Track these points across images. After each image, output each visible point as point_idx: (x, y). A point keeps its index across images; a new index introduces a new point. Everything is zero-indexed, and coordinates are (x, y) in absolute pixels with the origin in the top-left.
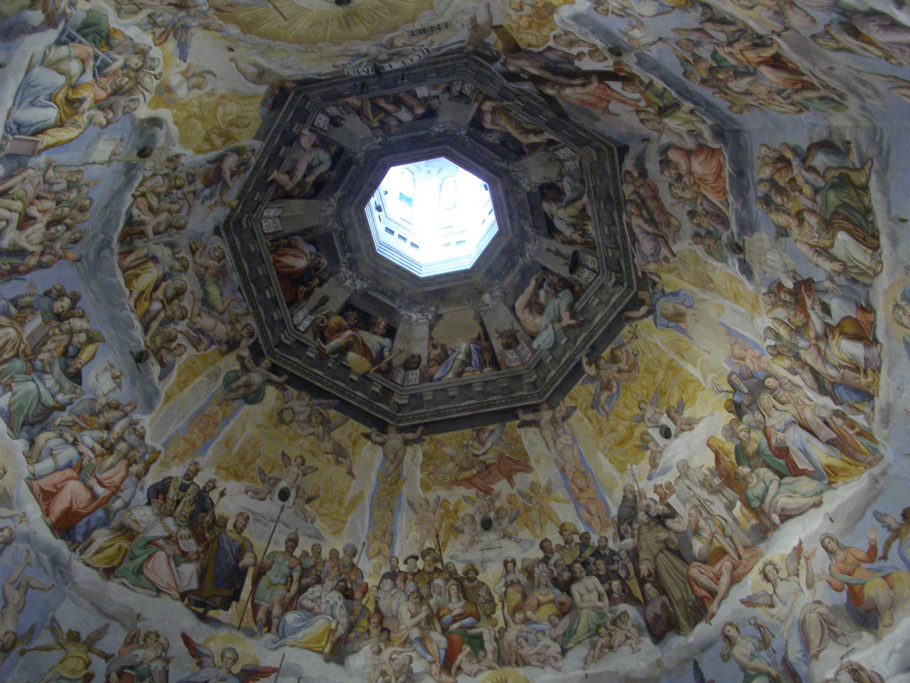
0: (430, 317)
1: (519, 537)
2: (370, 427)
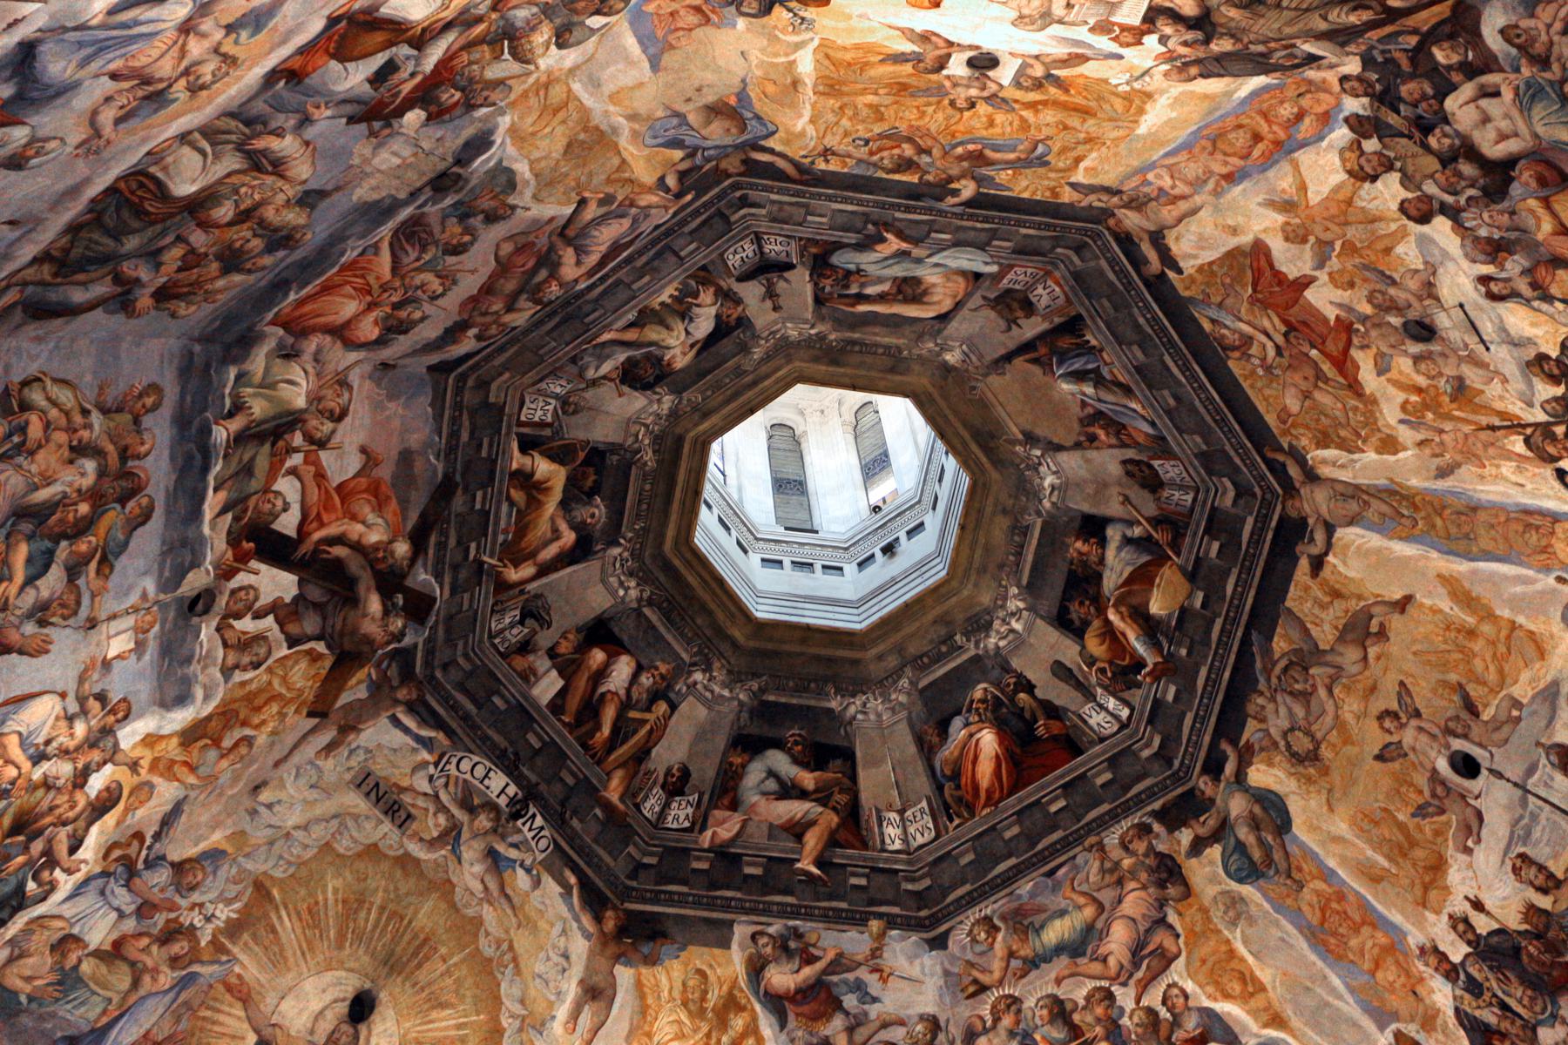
0: (1038, 453)
1: (1421, 267)
2: (1295, 560)
